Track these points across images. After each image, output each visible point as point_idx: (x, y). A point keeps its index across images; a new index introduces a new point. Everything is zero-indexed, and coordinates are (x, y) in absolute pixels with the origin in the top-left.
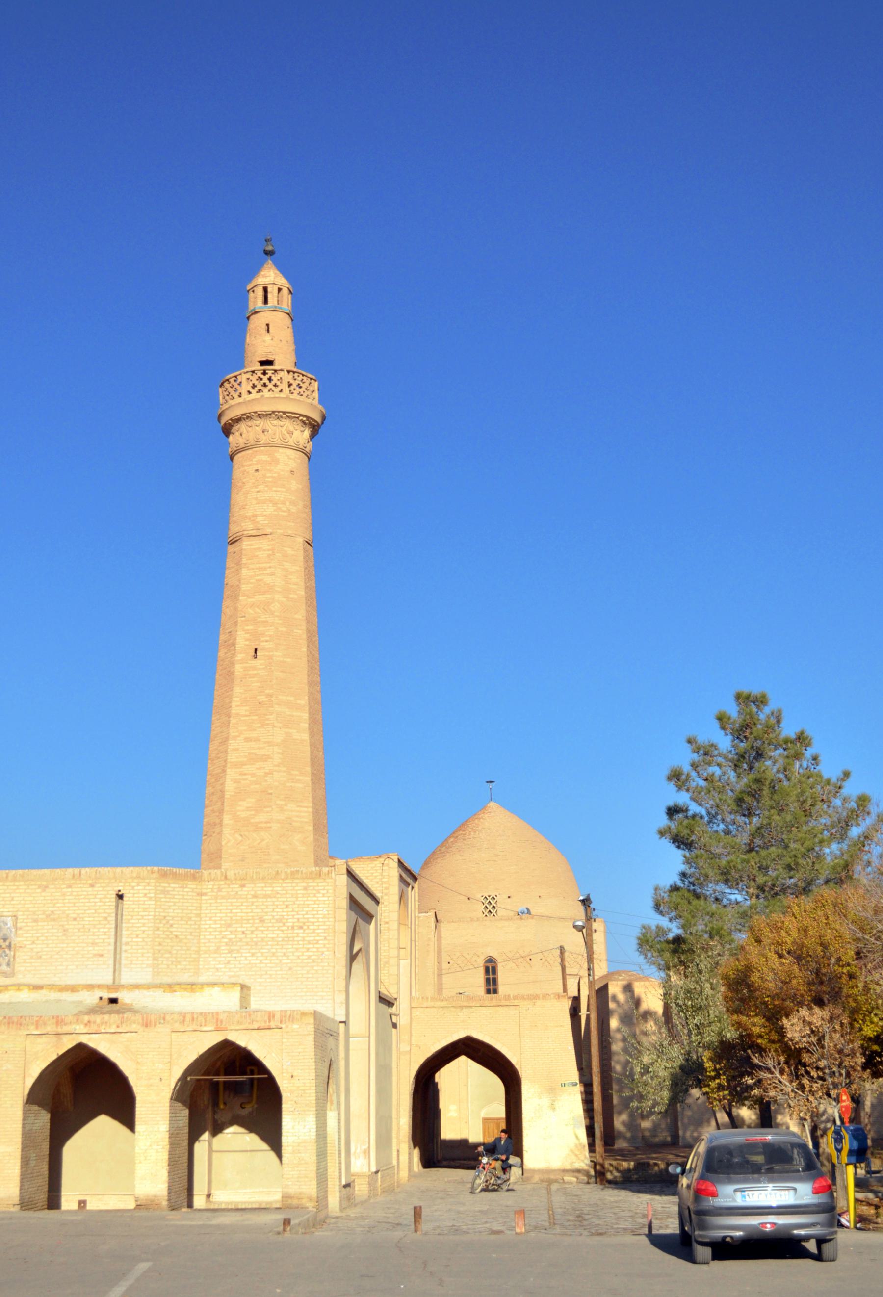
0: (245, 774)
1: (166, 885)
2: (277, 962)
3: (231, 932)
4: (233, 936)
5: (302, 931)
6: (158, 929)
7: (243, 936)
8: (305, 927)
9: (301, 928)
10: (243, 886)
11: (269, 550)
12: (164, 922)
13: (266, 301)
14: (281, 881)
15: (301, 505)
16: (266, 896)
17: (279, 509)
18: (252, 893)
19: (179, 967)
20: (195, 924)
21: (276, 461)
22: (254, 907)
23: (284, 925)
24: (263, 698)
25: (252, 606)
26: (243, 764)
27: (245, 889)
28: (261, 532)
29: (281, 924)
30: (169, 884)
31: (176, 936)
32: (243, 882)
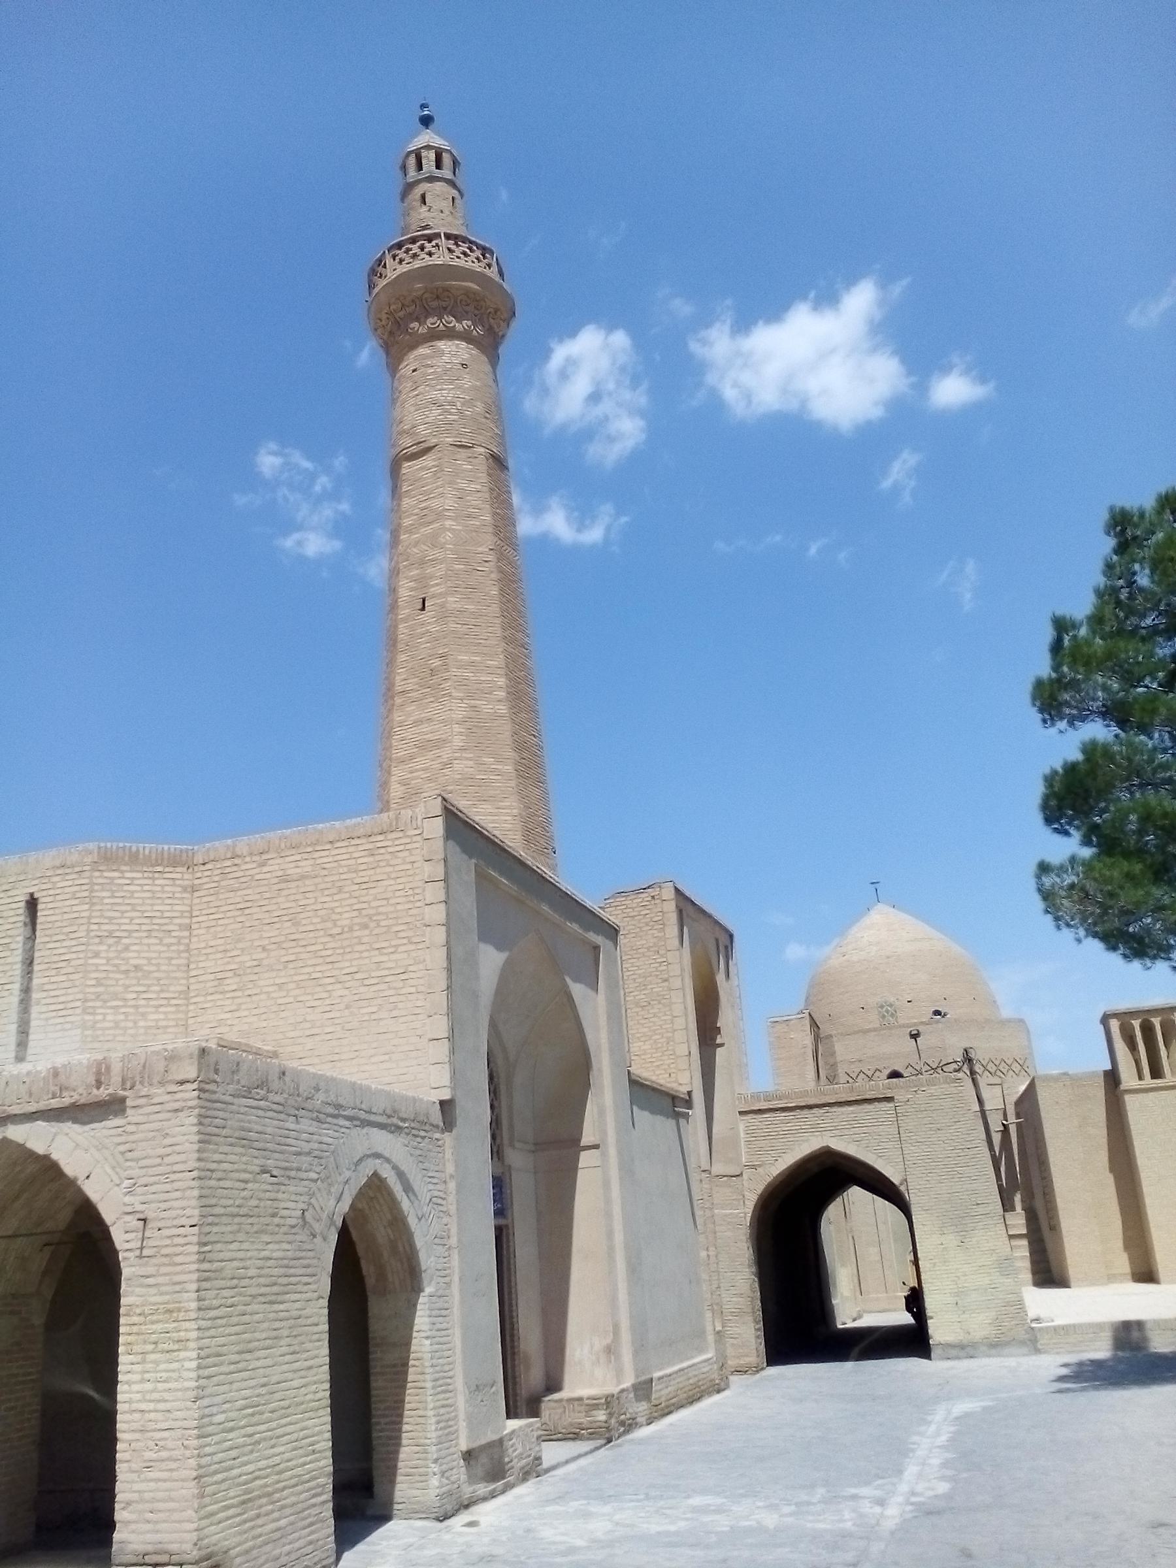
0: (417, 771)
1: (116, 874)
2: (325, 995)
3: (243, 950)
4: (247, 958)
5: (367, 932)
6: (97, 955)
7: (264, 955)
8: (372, 925)
9: (366, 927)
10: (263, 864)
11: (434, 466)
12: (111, 941)
13: (420, 167)
14: (328, 846)
15: (479, 407)
16: (303, 877)
17: (446, 411)
18: (280, 873)
19: (141, 1024)
20: (179, 943)
21: (443, 353)
22: (280, 900)
23: (335, 925)
24: (436, 663)
25: (417, 544)
26: (412, 757)
27: (265, 869)
28: (424, 445)
29: (329, 924)
30: (122, 872)
31: (136, 967)
32: (265, 857)
